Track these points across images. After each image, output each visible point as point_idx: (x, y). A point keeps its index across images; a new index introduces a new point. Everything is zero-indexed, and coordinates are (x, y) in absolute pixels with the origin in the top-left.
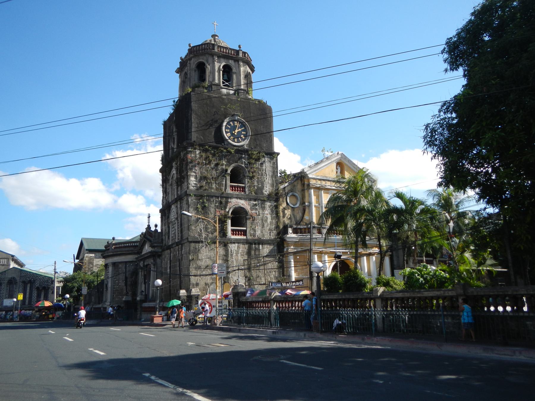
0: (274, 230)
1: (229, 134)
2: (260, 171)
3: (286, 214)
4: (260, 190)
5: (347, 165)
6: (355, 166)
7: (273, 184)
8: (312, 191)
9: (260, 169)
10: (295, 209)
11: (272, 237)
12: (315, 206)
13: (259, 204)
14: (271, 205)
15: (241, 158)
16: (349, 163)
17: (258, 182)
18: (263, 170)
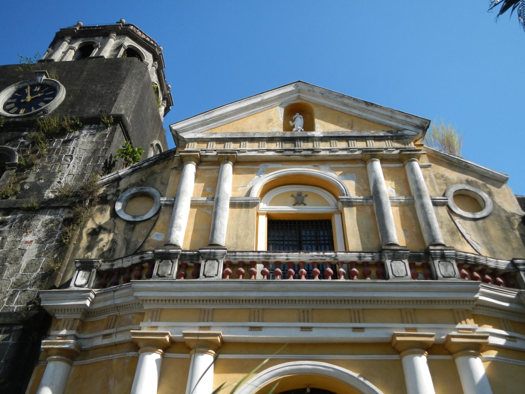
0: (32, 285)
1: (14, 104)
2: (57, 153)
3: (102, 240)
4: (38, 189)
5: (318, 105)
6: (346, 101)
7: (82, 175)
8: (191, 169)
9: (60, 149)
10: (138, 228)
11: (15, 307)
12: (194, 204)
13: (14, 220)
14: (52, 221)
15: (20, 137)
16: (327, 98)
17: (38, 175)
18: (66, 152)
